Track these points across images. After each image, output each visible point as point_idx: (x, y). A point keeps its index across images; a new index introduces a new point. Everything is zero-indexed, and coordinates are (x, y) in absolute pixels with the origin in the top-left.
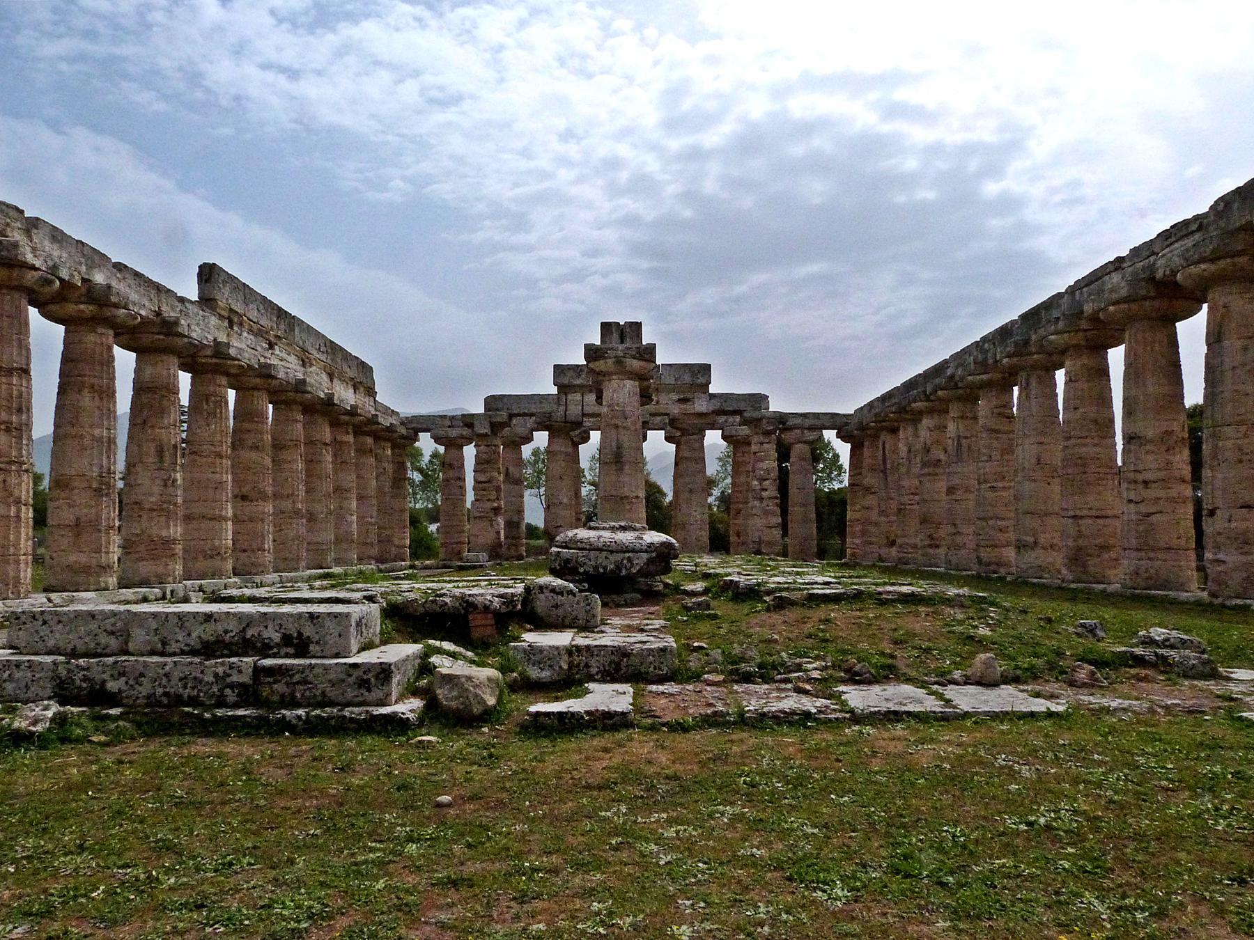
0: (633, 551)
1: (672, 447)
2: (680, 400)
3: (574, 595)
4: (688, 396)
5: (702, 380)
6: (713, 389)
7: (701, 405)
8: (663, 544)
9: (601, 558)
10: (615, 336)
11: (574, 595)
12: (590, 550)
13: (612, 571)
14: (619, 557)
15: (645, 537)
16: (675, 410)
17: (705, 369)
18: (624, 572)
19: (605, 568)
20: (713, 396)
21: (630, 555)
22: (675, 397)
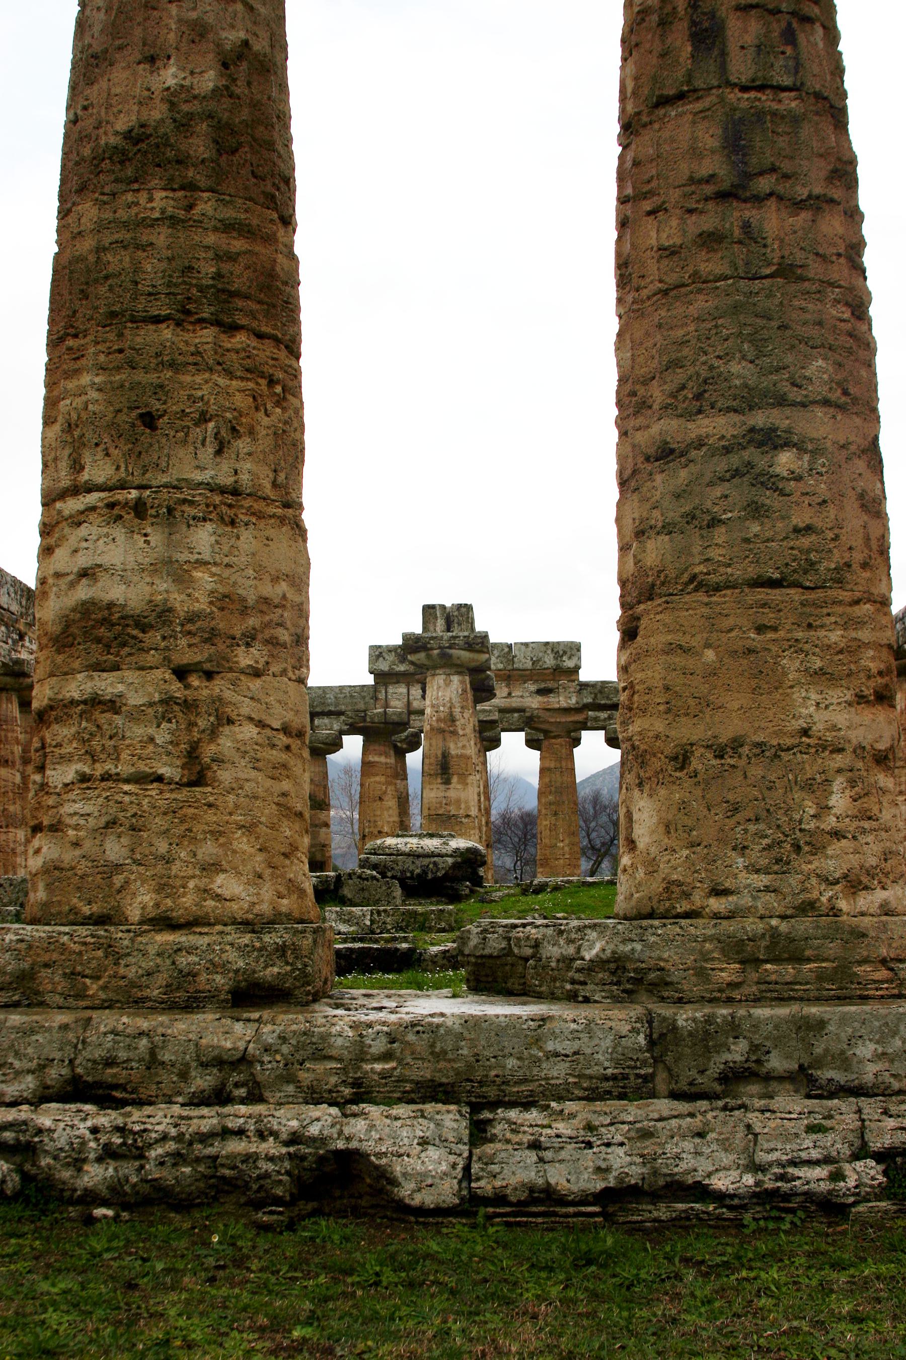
0: (439, 855)
1: (537, 754)
2: (540, 692)
3: (378, 880)
4: (550, 685)
5: (570, 664)
6: (585, 675)
7: (565, 699)
8: (468, 850)
9: (408, 864)
10: (440, 624)
11: (378, 880)
12: (398, 855)
13: (418, 875)
14: (426, 861)
15: (451, 843)
16: (534, 703)
17: (574, 649)
18: (430, 876)
19: (412, 872)
20: (584, 686)
21: (436, 859)
22: (533, 687)
